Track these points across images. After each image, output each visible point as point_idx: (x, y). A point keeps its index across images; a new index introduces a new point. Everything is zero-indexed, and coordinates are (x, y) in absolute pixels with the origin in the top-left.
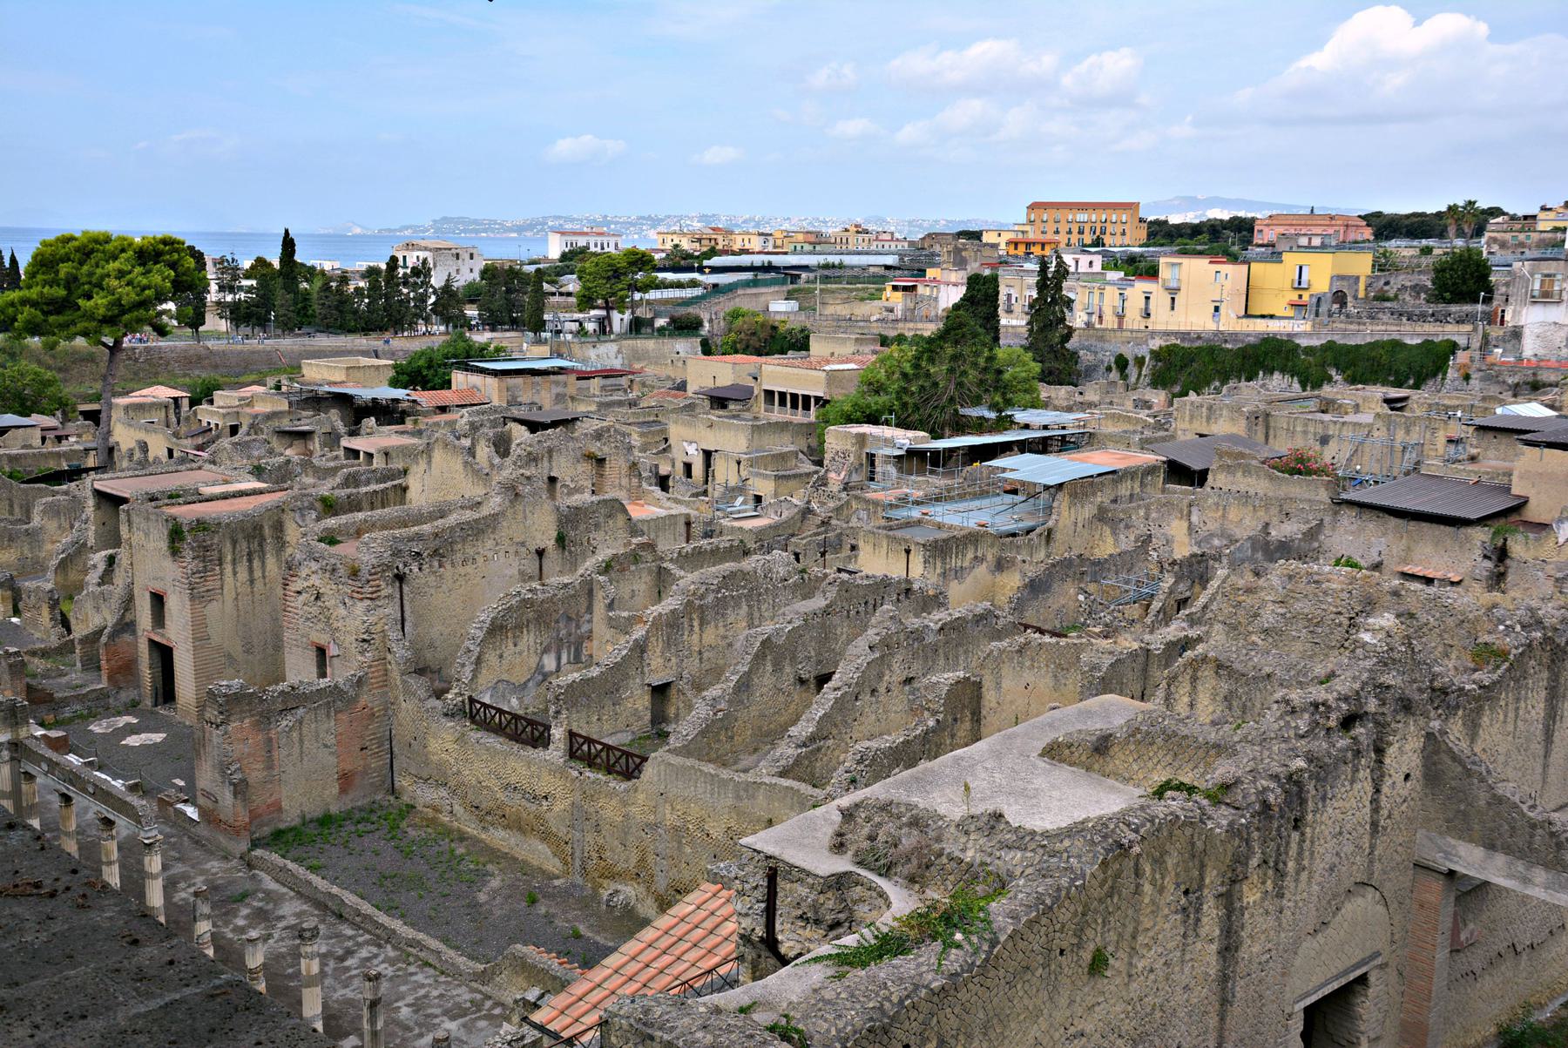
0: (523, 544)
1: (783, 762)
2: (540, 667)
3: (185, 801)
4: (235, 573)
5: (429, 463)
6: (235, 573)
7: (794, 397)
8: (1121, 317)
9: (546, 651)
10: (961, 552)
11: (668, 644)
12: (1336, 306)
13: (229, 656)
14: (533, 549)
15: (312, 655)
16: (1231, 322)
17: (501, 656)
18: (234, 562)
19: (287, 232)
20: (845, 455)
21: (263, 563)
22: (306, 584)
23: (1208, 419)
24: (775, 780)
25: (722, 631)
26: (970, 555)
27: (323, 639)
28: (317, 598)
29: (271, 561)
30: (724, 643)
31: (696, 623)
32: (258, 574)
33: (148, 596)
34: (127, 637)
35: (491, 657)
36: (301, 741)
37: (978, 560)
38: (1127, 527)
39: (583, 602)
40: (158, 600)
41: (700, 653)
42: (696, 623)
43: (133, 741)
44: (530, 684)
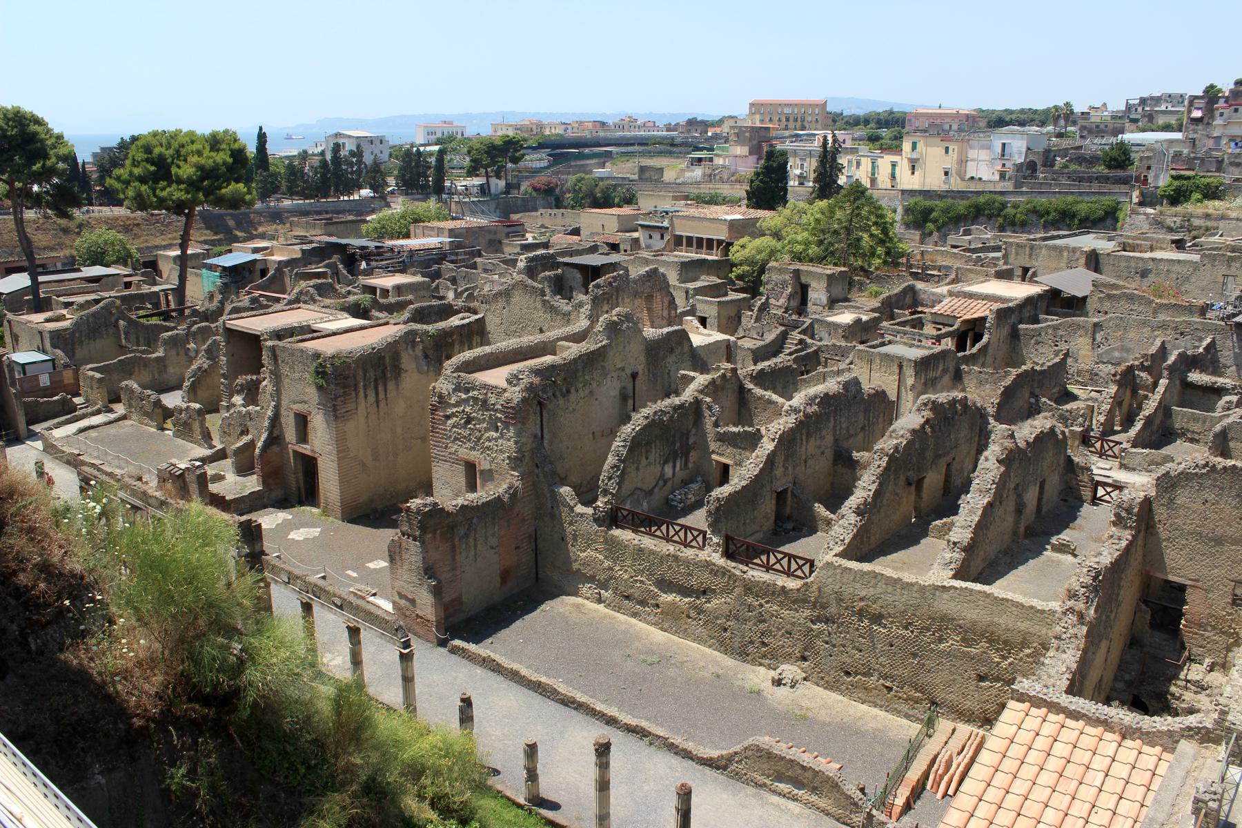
0: (623, 369)
1: (953, 566)
2: (662, 475)
3: (374, 595)
4: (366, 396)
5: (508, 302)
6: (366, 396)
7: (700, 240)
8: (873, 181)
9: (666, 462)
10: (936, 367)
11: (786, 460)
12: (1029, 172)
13: (363, 464)
14: (628, 372)
15: (461, 468)
16: (956, 184)
17: (638, 469)
18: (365, 387)
19: (261, 128)
20: (784, 284)
21: (386, 391)
22: (455, 410)
23: (1030, 255)
24: (958, 584)
25: (818, 442)
26: (941, 368)
27: (475, 456)
28: (469, 421)
29: (391, 385)
30: (819, 452)
31: (804, 437)
32: (382, 396)
33: (292, 416)
34: (275, 449)
35: (631, 469)
36: (476, 546)
37: (945, 371)
38: (1038, 343)
39: (691, 418)
40: (302, 421)
41: (806, 462)
42: (804, 437)
43: (297, 535)
44: (656, 490)
